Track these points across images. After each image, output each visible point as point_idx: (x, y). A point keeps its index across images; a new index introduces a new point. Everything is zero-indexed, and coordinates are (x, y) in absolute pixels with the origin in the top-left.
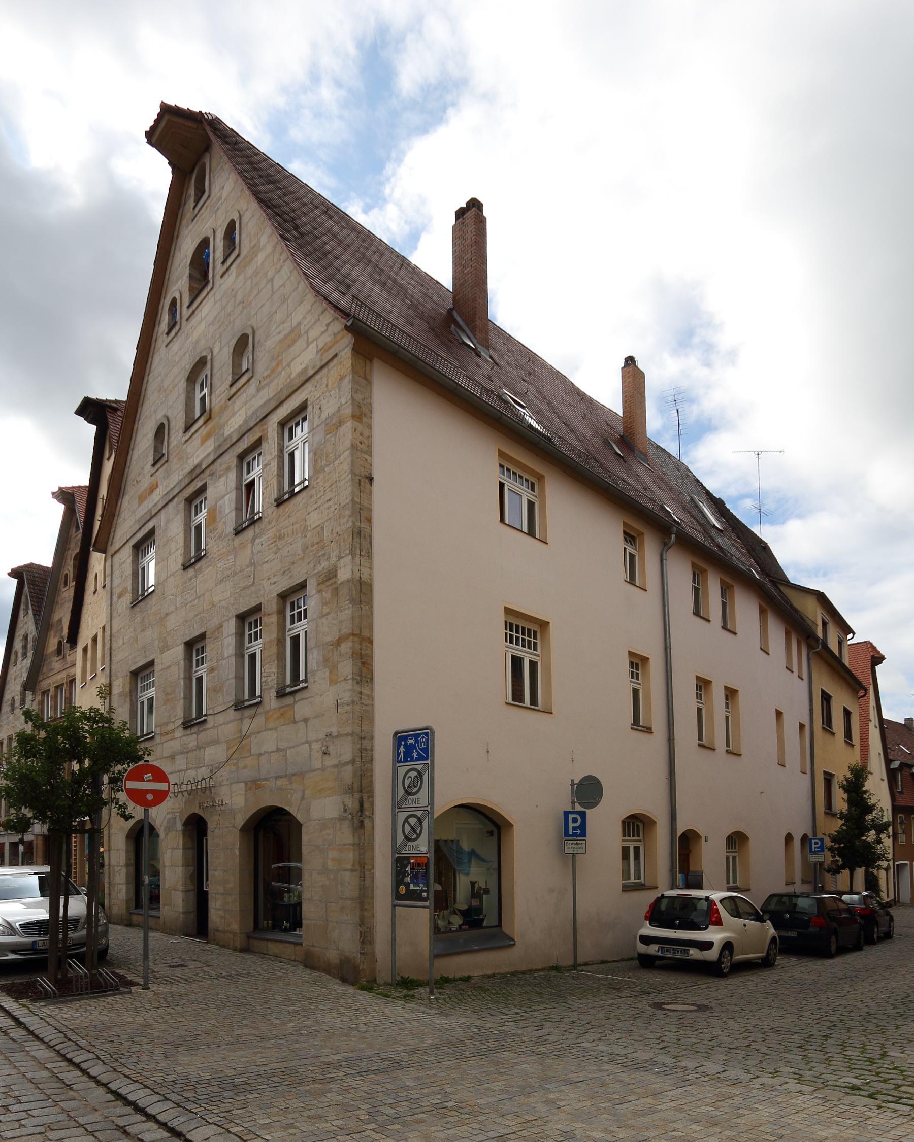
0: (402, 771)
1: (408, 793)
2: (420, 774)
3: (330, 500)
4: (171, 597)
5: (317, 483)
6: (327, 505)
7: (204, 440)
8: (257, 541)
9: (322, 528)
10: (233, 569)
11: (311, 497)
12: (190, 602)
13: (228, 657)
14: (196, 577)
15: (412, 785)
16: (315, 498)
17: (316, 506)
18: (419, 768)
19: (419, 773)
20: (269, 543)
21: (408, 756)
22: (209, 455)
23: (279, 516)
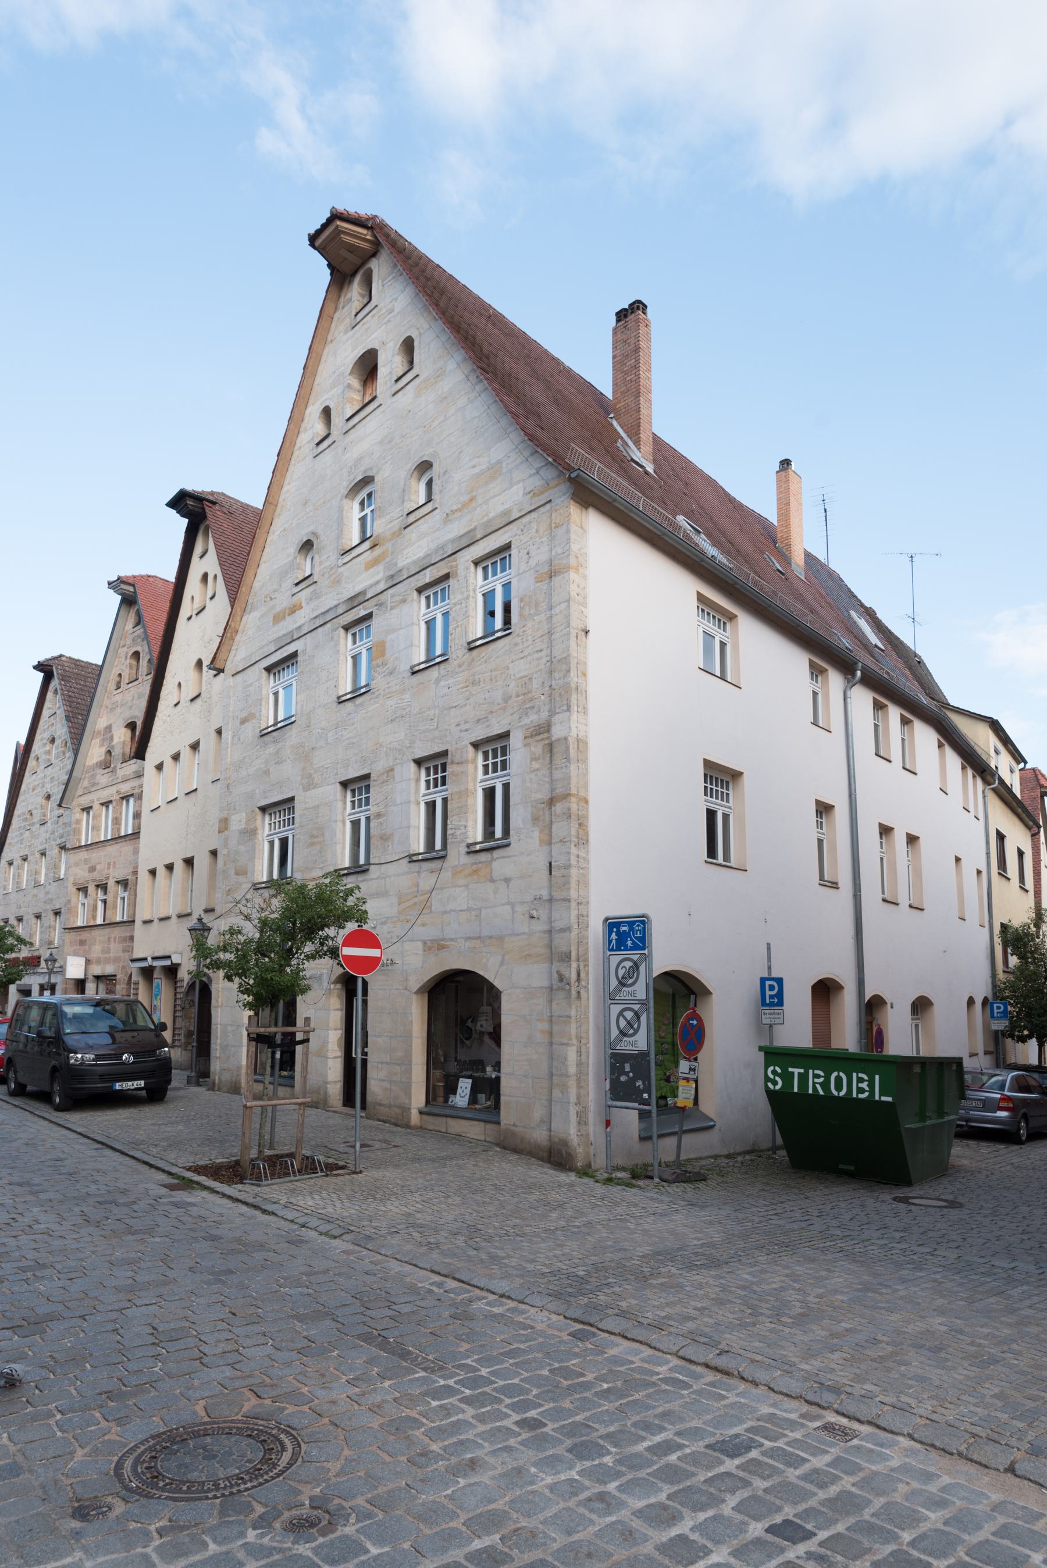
0: (615, 960)
1: (622, 984)
2: (636, 966)
3: (541, 651)
4: (320, 730)
5: (524, 631)
6: (536, 656)
7: (369, 565)
8: (442, 683)
9: (531, 679)
10: (408, 709)
11: (516, 645)
12: (348, 739)
14: (356, 712)
16: (521, 647)
17: (522, 655)
18: (635, 958)
19: (635, 963)
20: (459, 687)
21: (621, 945)
22: (378, 582)
23: (473, 660)
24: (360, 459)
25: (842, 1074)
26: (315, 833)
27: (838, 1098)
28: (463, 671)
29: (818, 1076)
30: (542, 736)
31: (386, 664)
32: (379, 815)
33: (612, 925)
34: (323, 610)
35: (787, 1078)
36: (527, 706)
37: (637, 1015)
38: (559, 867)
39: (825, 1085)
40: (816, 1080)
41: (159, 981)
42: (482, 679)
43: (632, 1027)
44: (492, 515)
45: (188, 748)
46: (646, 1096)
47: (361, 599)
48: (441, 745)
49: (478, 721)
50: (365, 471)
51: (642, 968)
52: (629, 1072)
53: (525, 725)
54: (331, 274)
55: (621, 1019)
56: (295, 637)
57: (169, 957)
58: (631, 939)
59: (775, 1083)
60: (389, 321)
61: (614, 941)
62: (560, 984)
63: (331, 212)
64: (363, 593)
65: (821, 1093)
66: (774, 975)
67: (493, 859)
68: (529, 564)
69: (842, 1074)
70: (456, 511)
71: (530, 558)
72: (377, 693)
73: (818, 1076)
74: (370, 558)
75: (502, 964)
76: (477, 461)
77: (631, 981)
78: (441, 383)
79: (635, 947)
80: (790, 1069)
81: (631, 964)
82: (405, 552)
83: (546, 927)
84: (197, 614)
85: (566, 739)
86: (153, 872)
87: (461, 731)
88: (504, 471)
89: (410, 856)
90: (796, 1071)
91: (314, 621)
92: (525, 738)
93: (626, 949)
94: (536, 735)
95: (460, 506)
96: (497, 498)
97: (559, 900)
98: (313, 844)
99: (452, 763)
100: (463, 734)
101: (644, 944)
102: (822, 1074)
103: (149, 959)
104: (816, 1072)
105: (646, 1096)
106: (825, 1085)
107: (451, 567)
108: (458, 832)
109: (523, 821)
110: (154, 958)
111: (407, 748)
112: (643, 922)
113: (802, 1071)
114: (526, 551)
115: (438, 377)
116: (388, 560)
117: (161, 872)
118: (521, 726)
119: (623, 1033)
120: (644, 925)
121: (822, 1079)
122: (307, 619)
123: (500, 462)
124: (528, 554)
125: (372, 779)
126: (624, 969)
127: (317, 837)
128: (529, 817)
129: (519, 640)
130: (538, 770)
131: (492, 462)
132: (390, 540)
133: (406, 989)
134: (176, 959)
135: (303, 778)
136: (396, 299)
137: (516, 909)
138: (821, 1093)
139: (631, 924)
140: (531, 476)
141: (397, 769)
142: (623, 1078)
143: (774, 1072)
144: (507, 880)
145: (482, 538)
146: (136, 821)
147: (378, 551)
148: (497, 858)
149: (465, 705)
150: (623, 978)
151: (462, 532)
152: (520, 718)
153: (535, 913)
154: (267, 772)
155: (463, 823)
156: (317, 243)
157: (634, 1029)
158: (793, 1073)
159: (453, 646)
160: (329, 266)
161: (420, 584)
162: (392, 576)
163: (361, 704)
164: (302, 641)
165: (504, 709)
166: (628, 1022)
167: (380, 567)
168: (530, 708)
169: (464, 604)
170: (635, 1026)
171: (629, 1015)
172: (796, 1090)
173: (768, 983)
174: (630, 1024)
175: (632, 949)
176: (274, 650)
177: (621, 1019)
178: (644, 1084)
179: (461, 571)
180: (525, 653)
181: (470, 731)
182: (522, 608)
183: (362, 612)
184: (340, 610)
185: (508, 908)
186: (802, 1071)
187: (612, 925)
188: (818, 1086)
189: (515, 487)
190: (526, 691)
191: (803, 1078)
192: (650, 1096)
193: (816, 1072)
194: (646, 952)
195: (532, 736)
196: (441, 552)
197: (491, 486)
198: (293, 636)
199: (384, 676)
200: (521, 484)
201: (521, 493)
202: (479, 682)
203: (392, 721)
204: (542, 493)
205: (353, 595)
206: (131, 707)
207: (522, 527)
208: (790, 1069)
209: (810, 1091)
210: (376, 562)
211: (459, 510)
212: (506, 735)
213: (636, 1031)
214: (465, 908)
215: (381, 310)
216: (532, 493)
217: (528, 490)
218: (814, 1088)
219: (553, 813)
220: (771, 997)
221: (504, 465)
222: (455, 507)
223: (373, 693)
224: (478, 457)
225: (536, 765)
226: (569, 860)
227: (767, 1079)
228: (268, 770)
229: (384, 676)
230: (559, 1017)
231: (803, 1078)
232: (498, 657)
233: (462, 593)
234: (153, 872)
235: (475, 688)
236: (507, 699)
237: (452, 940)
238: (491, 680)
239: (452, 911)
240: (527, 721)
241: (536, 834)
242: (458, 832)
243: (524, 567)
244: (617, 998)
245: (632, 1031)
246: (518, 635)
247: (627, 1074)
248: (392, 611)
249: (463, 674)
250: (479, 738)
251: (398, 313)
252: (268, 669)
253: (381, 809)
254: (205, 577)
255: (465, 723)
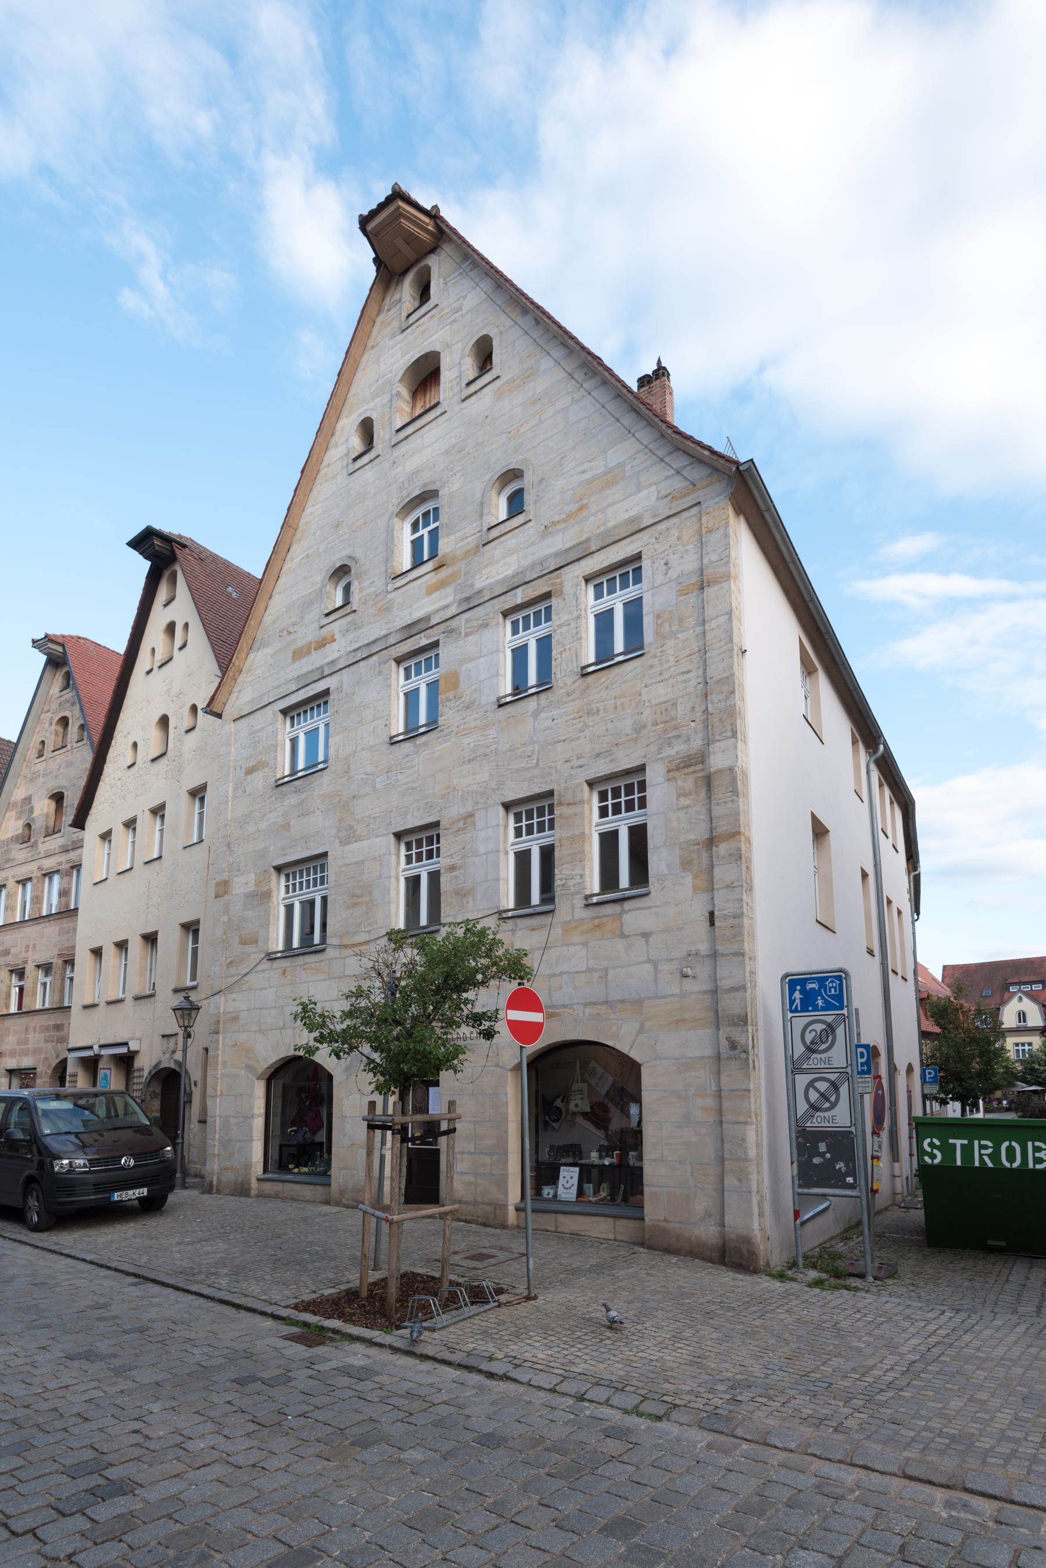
0: (800, 1023)
1: (811, 1049)
2: (831, 1029)
3: (688, 672)
4: (363, 776)
5: (662, 652)
6: (681, 678)
7: (431, 590)
8: (543, 715)
9: (674, 705)
10: (493, 747)
11: (651, 667)
12: (405, 784)
13: (486, 854)
14: (417, 753)
15: (817, 1040)
16: (659, 669)
17: (660, 678)
18: (829, 1019)
19: (829, 1025)
20: (568, 718)
21: (808, 1002)
22: (447, 607)
23: (588, 687)
24: (416, 473)
25: (1014, 1144)
26: (358, 892)
27: (1011, 1169)
28: (574, 700)
29: (986, 1147)
30: (692, 769)
31: (461, 698)
32: (452, 868)
33: (794, 983)
34: (366, 642)
35: (948, 1151)
36: (670, 735)
37: (835, 1086)
38: (725, 917)
39: (995, 1156)
40: (983, 1152)
41: (108, 1072)
42: (601, 708)
43: (827, 1099)
44: (610, 524)
45: (148, 813)
46: (850, 1180)
47: (422, 626)
48: (543, 785)
49: (598, 755)
50: (425, 485)
51: (840, 1031)
52: (825, 1153)
53: (668, 757)
54: (378, 271)
55: (811, 1091)
56: (326, 673)
57: (126, 1044)
58: (823, 998)
59: (933, 1156)
60: (455, 321)
61: (798, 1001)
62: (731, 1053)
63: (393, 189)
64: (427, 618)
65: (990, 1165)
66: (863, 1042)
67: (623, 912)
68: (669, 575)
69: (1014, 1144)
70: (559, 522)
71: (669, 569)
72: (447, 731)
73: (986, 1147)
74: (434, 581)
75: (641, 1031)
76: (586, 466)
77: (824, 1046)
78: (532, 383)
79: (828, 1007)
80: (951, 1141)
81: (824, 1027)
82: (485, 571)
83: (707, 987)
84: (160, 667)
85: (731, 769)
86: (97, 952)
87: (572, 767)
88: (627, 475)
89: (500, 912)
90: (958, 1143)
91: (353, 654)
92: (669, 771)
93: (816, 1009)
94: (685, 767)
95: (564, 516)
96: (618, 505)
97: (727, 955)
98: (354, 905)
99: (560, 804)
100: (575, 771)
101: (841, 1002)
102: (990, 1144)
103: (96, 1047)
104: (983, 1142)
105: (850, 1180)
106: (995, 1156)
107: (553, 584)
108: (571, 883)
109: (668, 866)
110: (101, 1046)
111: (493, 790)
112: (839, 978)
113: (965, 1142)
114: (664, 561)
115: (528, 377)
116: (460, 581)
117: (110, 953)
118: (663, 758)
119: (814, 1108)
120: (841, 981)
121: (990, 1151)
122: (343, 651)
123: (622, 465)
124: (666, 564)
125: (441, 827)
126: (814, 1033)
127: (362, 896)
128: (677, 861)
129: (656, 661)
130: (688, 807)
131: (610, 466)
132: (462, 559)
133: (497, 1065)
134: (134, 1046)
135: (339, 831)
136: (465, 297)
137: (660, 968)
138: (990, 1165)
139: (822, 981)
140: (667, 478)
141: (479, 815)
142: (816, 1160)
143: (931, 1145)
144: (646, 935)
145: (598, 550)
146: (63, 899)
147: (444, 573)
148: (629, 911)
149: (578, 738)
150: (812, 1043)
151: (568, 545)
152: (661, 749)
153: (689, 971)
154: (286, 827)
155: (578, 871)
156: (370, 227)
157: (830, 1102)
158: (955, 1145)
159: (558, 673)
160: (377, 261)
161: (507, 606)
162: (468, 599)
163: (426, 744)
164: (336, 677)
165: (636, 740)
166: (822, 1095)
167: (450, 590)
168: (674, 737)
169: (573, 625)
170: (833, 1099)
171: (823, 1086)
172: (959, 1163)
173: (860, 1050)
174: (824, 1096)
175: (823, 1009)
176: (295, 689)
177: (811, 1091)
178: (847, 1165)
179: (568, 588)
180: (666, 675)
181: (585, 768)
182: (659, 626)
183: (423, 641)
184: (392, 640)
185: (648, 967)
186: (965, 1142)
187: (794, 983)
188: (986, 1158)
189: (645, 492)
190: (667, 719)
191: (967, 1150)
192: (855, 1179)
193: (983, 1142)
194: (845, 1012)
195: (678, 769)
196: (539, 568)
197: (609, 492)
198: (323, 672)
199: (458, 711)
200: (654, 488)
201: (654, 498)
202: (598, 711)
203: (469, 761)
204: (687, 495)
205: (409, 622)
206: (56, 777)
207: (657, 535)
208: (951, 1141)
209: (977, 1164)
210: (442, 584)
211: (564, 521)
212: (641, 769)
213: (834, 1105)
214: (584, 969)
215: (442, 309)
216: (670, 497)
217: (664, 493)
218: (981, 1160)
219: (714, 855)
220: (862, 1064)
221: (627, 468)
222: (557, 518)
223: (442, 731)
224: (589, 461)
225: (685, 802)
226: (741, 907)
227: (921, 1152)
228: (288, 824)
229: (458, 711)
230: (732, 1091)
231: (967, 1150)
232: (625, 682)
233: (571, 613)
234: (97, 952)
235: (591, 718)
236: (639, 728)
237: (564, 1006)
238: (616, 708)
239: (562, 973)
240: (670, 752)
241: (688, 879)
242: (571, 883)
243: (660, 579)
244: (805, 1066)
245: (827, 1105)
246: (655, 656)
247: (822, 1155)
248: (468, 638)
249: (571, 704)
250: (600, 775)
251: (468, 312)
252: (285, 712)
253: (456, 860)
254: (171, 628)
255: (578, 758)
